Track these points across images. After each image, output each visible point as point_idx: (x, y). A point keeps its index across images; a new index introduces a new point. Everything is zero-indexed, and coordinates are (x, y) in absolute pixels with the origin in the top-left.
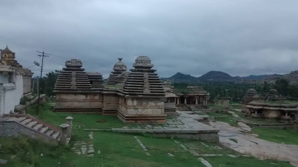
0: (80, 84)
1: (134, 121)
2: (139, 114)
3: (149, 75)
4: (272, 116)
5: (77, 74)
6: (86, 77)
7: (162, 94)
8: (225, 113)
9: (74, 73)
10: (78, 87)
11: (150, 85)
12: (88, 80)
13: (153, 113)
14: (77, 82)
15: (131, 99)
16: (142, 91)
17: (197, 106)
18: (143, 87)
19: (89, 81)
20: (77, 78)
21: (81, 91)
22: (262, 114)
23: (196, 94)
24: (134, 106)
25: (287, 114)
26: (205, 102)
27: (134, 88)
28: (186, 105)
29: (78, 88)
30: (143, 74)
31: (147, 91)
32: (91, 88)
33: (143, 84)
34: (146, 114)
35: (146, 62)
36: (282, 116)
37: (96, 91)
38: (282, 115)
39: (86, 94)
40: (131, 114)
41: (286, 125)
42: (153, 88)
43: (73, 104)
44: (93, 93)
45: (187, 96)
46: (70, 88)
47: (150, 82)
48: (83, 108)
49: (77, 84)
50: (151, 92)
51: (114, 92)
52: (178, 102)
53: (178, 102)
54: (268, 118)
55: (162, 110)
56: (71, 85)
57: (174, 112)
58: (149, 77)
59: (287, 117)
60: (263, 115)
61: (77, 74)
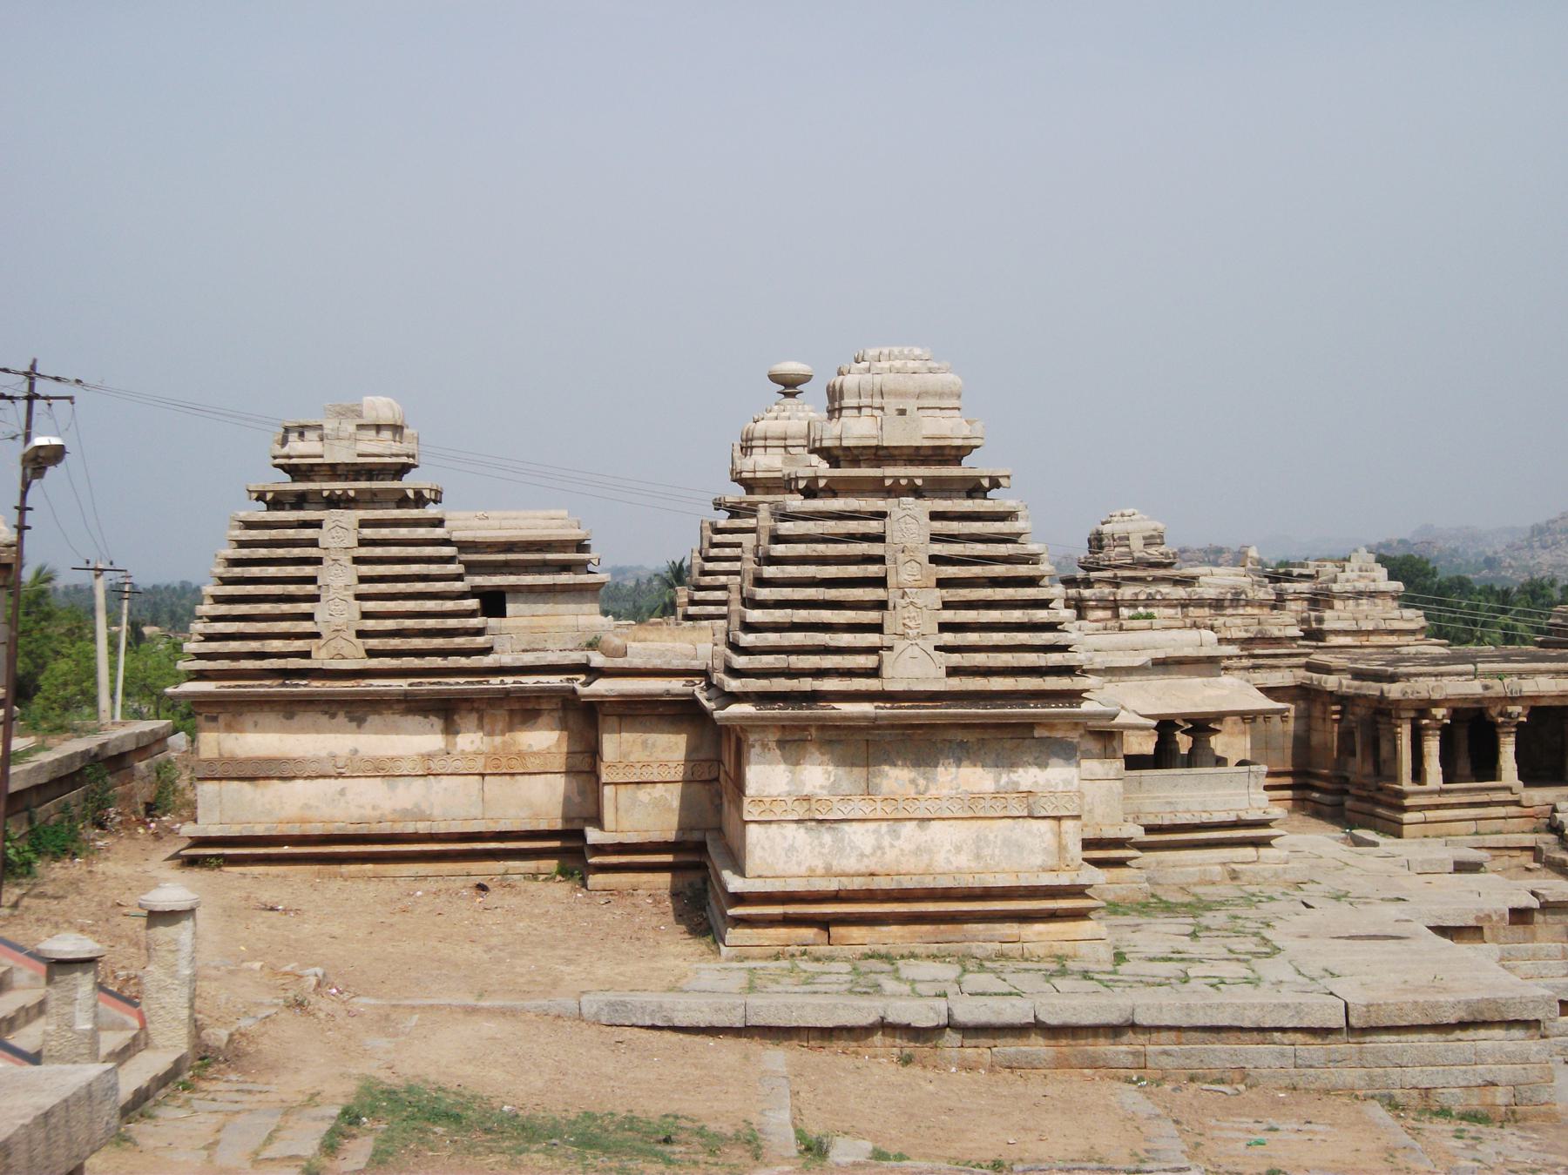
0: (390, 624)
1: (808, 933)
2: (850, 863)
3: (935, 516)
5: (368, 533)
6: (449, 560)
7: (1052, 683)
9: (339, 531)
10: (374, 643)
11: (947, 605)
12: (458, 586)
13: (978, 857)
14: (370, 606)
15: (772, 737)
16: (868, 661)
18: (877, 628)
19: (462, 596)
20: (366, 570)
21: (402, 684)
24: (807, 799)
27: (797, 638)
28: (1509, 789)
29: (371, 653)
30: (881, 515)
31: (915, 664)
32: (487, 651)
33: (882, 605)
34: (910, 864)
35: (911, 405)
37: (529, 681)
39: (446, 710)
40: (780, 868)
42: (972, 638)
43: (342, 792)
44: (505, 695)
45: (1516, 709)
46: (306, 655)
47: (942, 583)
48: (422, 827)
49: (370, 624)
50: (953, 672)
51: (677, 685)
52: (1433, 767)
53: (1433, 767)
55: (1059, 834)
56: (317, 635)
57: (1249, 852)
58: (936, 538)
61: (368, 533)
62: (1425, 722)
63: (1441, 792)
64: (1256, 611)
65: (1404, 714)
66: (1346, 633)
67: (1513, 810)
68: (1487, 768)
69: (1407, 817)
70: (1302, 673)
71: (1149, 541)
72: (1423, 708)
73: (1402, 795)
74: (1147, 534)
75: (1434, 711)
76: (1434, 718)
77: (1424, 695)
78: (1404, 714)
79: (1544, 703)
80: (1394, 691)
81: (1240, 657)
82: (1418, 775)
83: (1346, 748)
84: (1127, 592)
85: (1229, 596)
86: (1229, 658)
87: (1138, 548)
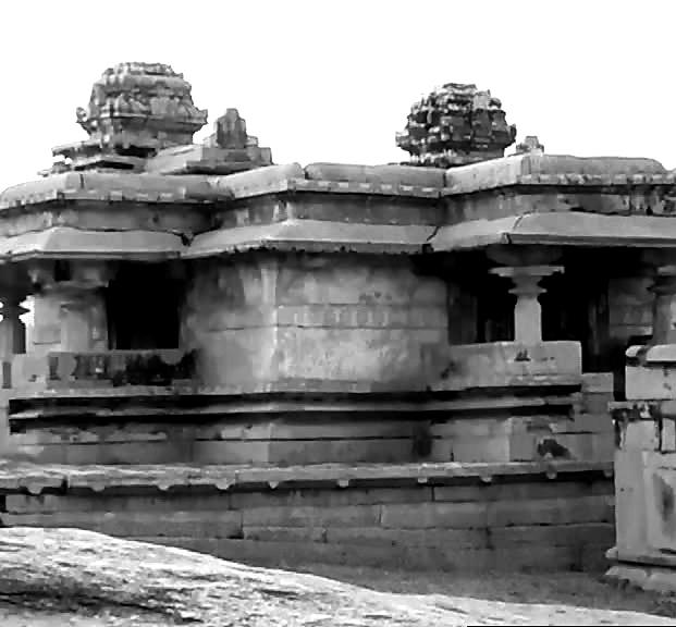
4: (318, 373)
22: (171, 356)
25: (528, 316)
36: (457, 352)
38: (456, 335)
41: (502, 479)
54: (243, 409)
59: (530, 351)
60: (190, 365)
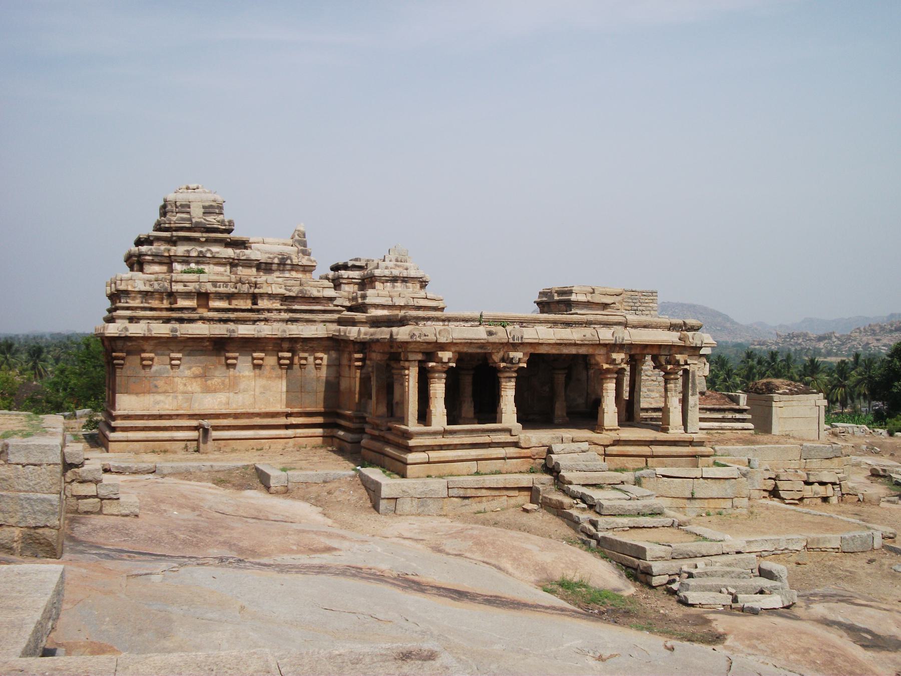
8: (829, 491)
17: (617, 443)
23: (606, 335)
26: (684, 402)
28: (509, 431)
45: (517, 355)
62: (431, 364)
63: (445, 433)
64: (300, 275)
65: (412, 357)
66: (383, 307)
67: (512, 451)
68: (488, 411)
69: (411, 457)
70: (334, 327)
71: (208, 210)
72: (430, 350)
73: (408, 435)
74: (207, 204)
75: (440, 354)
76: (440, 361)
77: (431, 338)
78: (412, 357)
79: (543, 350)
80: (402, 333)
81: (279, 311)
82: (424, 416)
83: (365, 392)
84: (180, 250)
85: (276, 261)
86: (269, 310)
87: (197, 214)
